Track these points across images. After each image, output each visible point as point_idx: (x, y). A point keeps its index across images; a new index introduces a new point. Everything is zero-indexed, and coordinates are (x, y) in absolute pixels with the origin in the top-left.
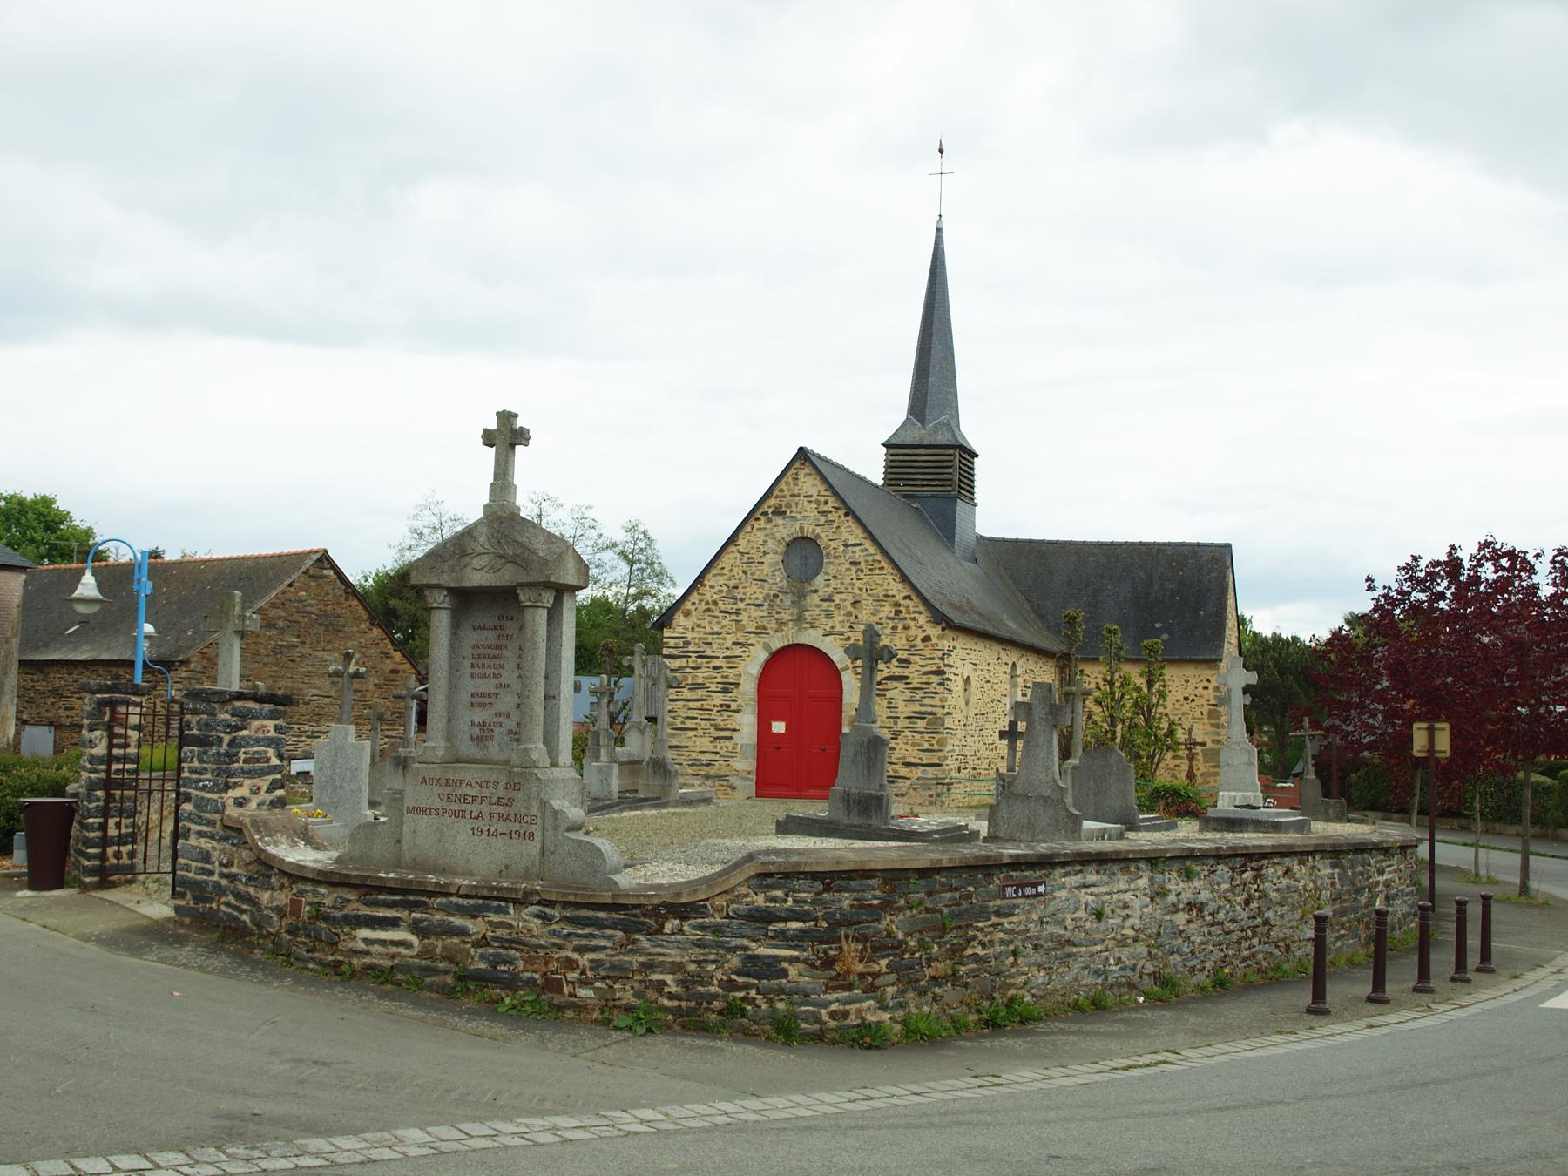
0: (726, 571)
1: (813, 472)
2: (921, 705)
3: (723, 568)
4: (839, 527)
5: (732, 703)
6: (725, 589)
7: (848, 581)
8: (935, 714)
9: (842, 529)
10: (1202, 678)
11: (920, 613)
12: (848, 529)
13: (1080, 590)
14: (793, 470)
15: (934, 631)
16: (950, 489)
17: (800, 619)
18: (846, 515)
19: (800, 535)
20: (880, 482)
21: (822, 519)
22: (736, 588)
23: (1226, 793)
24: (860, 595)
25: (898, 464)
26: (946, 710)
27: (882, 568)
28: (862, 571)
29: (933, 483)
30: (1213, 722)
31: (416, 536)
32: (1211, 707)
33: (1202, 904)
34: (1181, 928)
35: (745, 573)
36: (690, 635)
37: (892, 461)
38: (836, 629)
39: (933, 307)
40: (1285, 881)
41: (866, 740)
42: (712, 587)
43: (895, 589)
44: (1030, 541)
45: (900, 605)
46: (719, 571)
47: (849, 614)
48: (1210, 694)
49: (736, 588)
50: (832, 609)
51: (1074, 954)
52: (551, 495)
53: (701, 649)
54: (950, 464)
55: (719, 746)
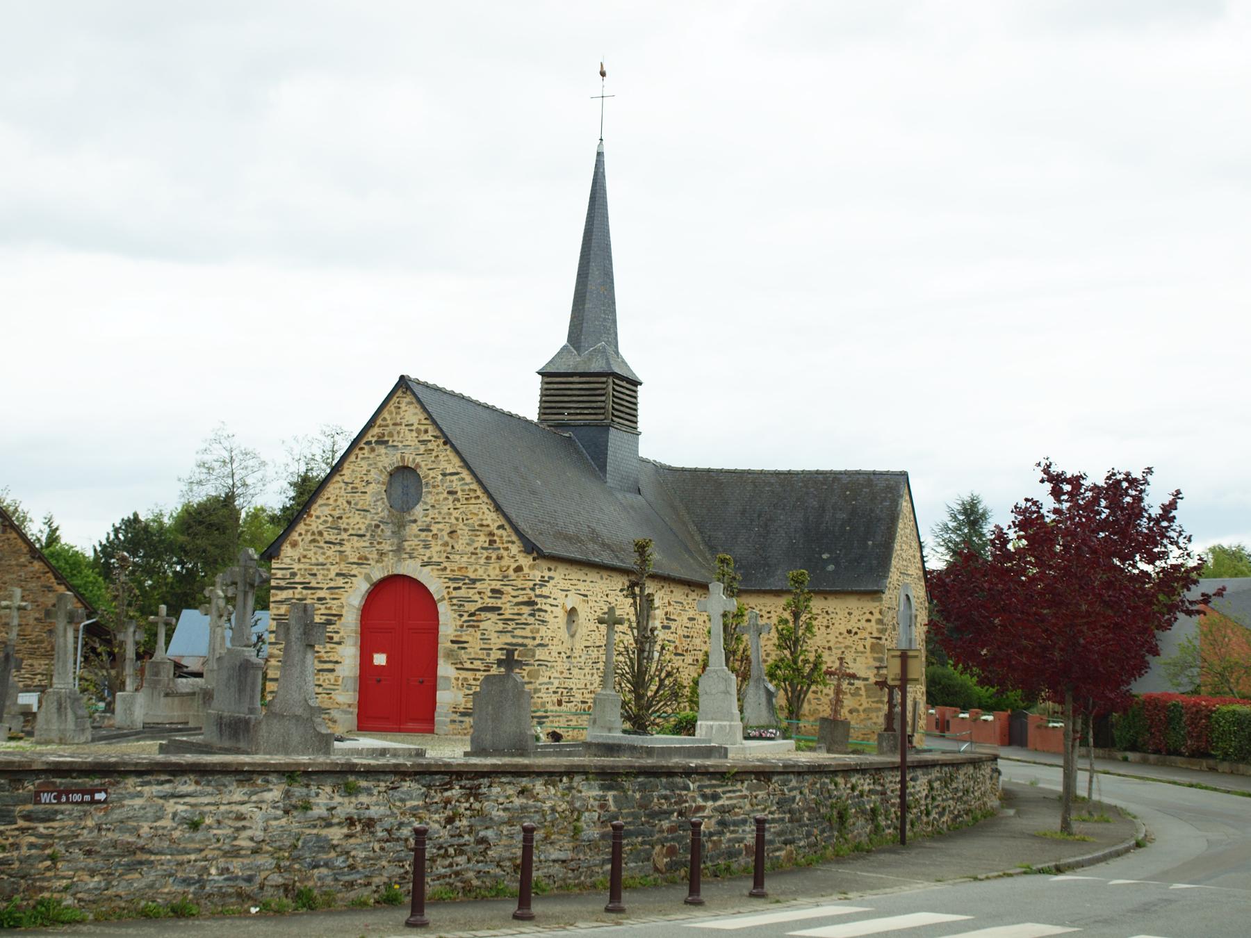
0: (331, 501)
1: (414, 400)
2: (513, 637)
3: (328, 498)
4: (438, 456)
6: (330, 519)
7: (445, 510)
8: (526, 646)
9: (441, 457)
10: (864, 610)
11: (513, 542)
12: (446, 458)
13: (752, 520)
14: (395, 399)
15: (525, 561)
16: (602, 417)
17: (399, 550)
18: (445, 443)
19: (401, 464)
20: (532, 414)
21: (422, 448)
22: (340, 518)
23: (704, 723)
24: (457, 525)
25: (552, 392)
26: (538, 641)
27: (478, 497)
28: (458, 500)
29: (586, 412)
30: (876, 655)
31: (205, 471)
32: (874, 641)
33: (371, 819)
34: (335, 842)
35: (349, 503)
36: (296, 566)
37: (546, 389)
38: (433, 560)
39: (592, 232)
40: (518, 802)
41: (238, 664)
42: (318, 517)
43: (489, 518)
44: (709, 471)
45: (494, 535)
46: (325, 502)
47: (446, 544)
48: (873, 626)
49: (340, 518)
50: (430, 539)
51: (152, 862)
52: (345, 429)
53: (307, 581)
54: (603, 392)
55: (322, 679)
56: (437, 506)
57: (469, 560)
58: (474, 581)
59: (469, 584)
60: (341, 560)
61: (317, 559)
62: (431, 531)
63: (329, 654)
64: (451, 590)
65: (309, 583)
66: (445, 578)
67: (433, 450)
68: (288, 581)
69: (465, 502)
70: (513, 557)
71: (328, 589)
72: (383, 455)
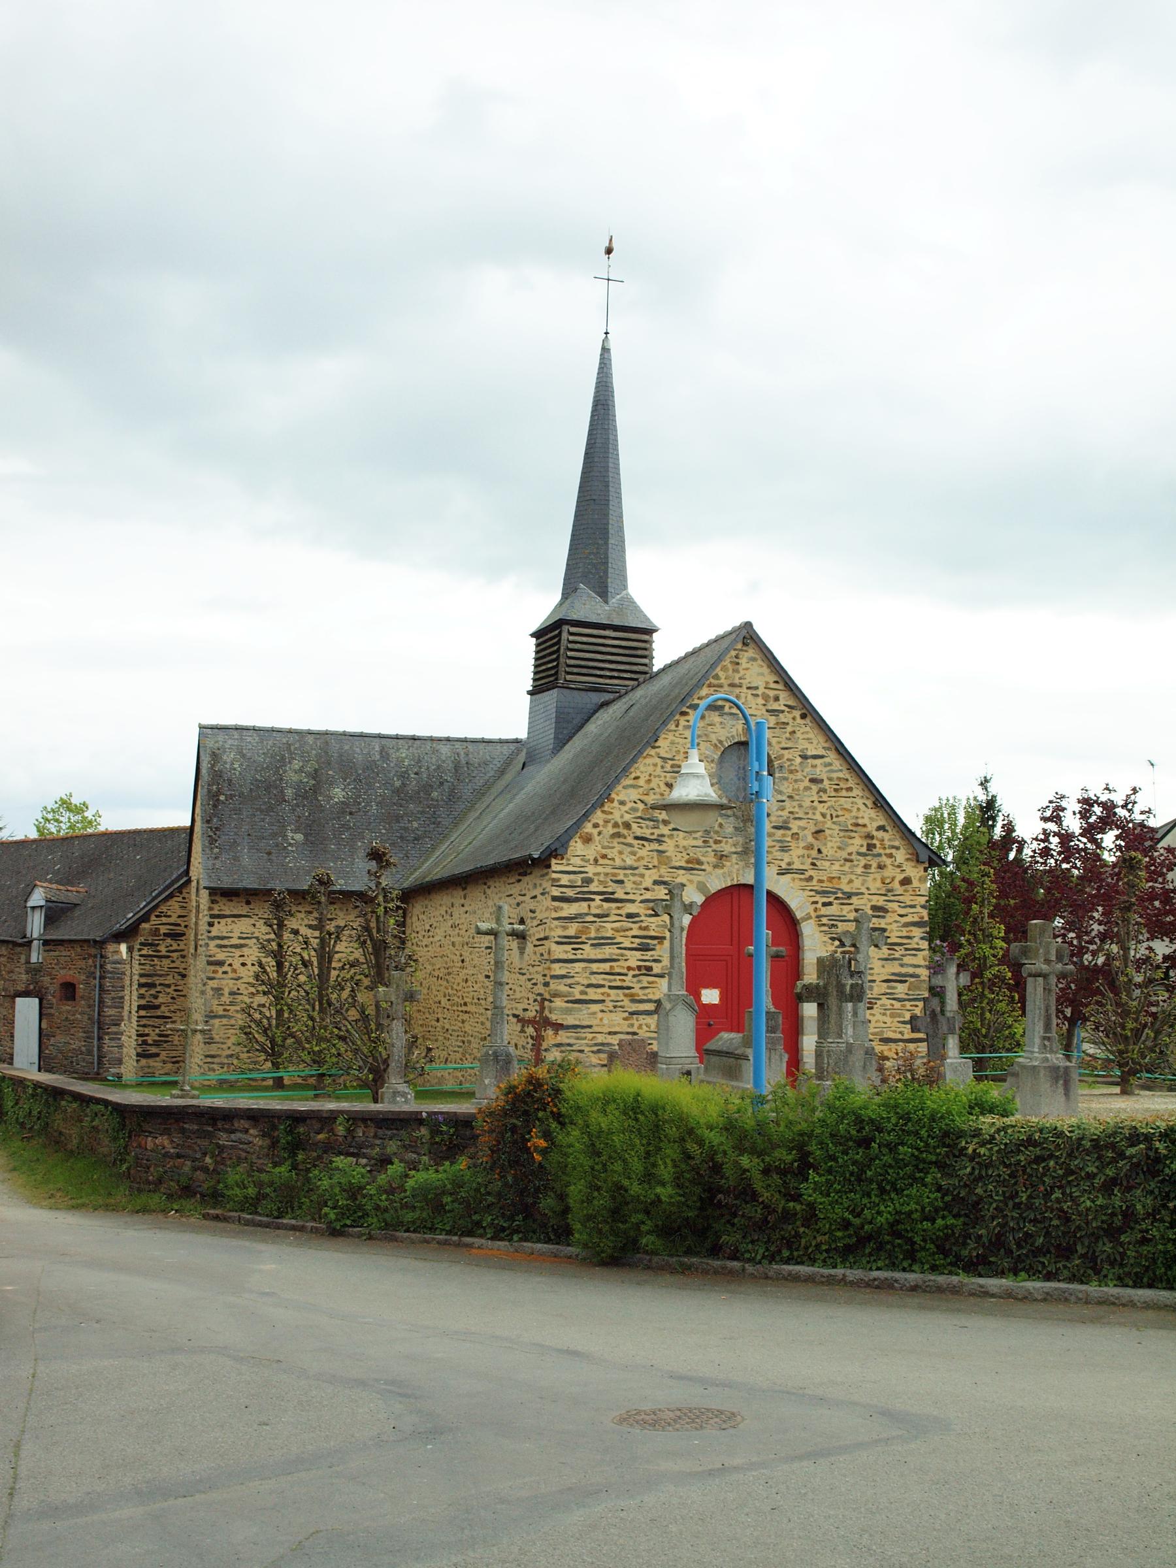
0: (641, 782)
2: (902, 966)
3: (636, 778)
4: (794, 732)
5: (654, 965)
6: (641, 806)
7: (807, 803)
8: (917, 976)
9: (798, 734)
11: (897, 848)
21: (772, 720)
27: (850, 789)
28: (825, 791)
29: (625, 675)
36: (591, 870)
42: (622, 803)
43: (866, 816)
45: (872, 837)
47: (810, 847)
50: (789, 839)
53: (610, 890)
55: (636, 1024)
56: (797, 797)
57: (842, 869)
58: (849, 896)
59: (842, 898)
60: (660, 862)
61: (624, 861)
62: (789, 829)
63: (647, 991)
64: (819, 905)
65: (613, 893)
66: (811, 890)
67: (788, 724)
68: (579, 889)
69: (833, 794)
70: (899, 866)
71: (641, 902)
72: (718, 725)
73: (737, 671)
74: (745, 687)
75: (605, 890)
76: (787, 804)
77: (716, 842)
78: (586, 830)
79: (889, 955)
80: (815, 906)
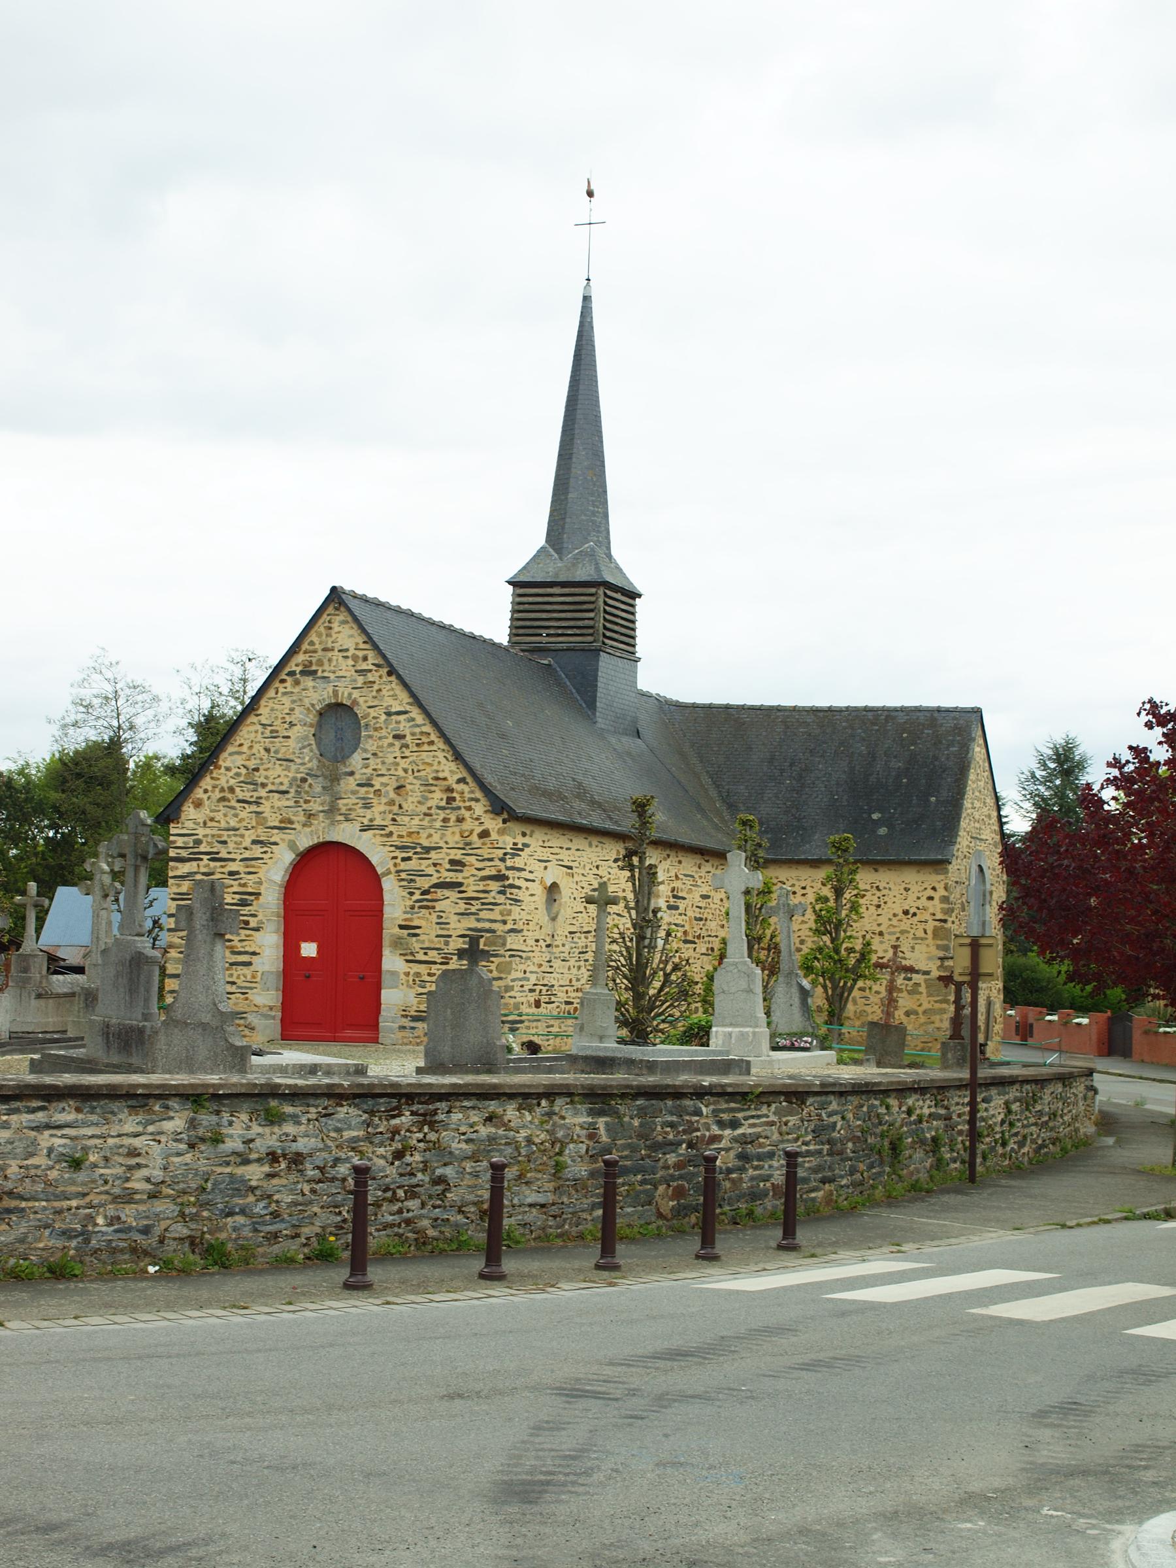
0: (245, 749)
1: (349, 619)
2: (478, 920)
3: (241, 745)
4: (380, 690)
5: (250, 919)
6: (243, 771)
7: (390, 760)
8: (494, 931)
9: (384, 692)
10: (925, 885)
11: (477, 800)
12: (391, 693)
13: (782, 771)
14: (325, 617)
15: (493, 824)
16: (590, 639)
17: (332, 810)
18: (390, 674)
19: (333, 701)
20: (501, 635)
21: (360, 680)
22: (257, 770)
23: (720, 1029)
24: (405, 778)
25: (527, 607)
26: (509, 926)
27: (431, 743)
28: (407, 746)
29: (569, 632)
30: (940, 942)
31: (82, 709)
32: (937, 923)
33: (299, 1154)
34: (253, 1183)
35: (267, 750)
36: (201, 832)
37: (519, 603)
38: (376, 823)
39: (576, 400)
40: (484, 1131)
41: (128, 957)
42: (228, 769)
43: (447, 769)
44: (727, 707)
45: (452, 790)
46: (237, 749)
47: (391, 803)
48: (936, 906)
49: (257, 770)
51: (23, 1210)
52: (258, 653)
53: (215, 850)
54: (591, 606)
55: (235, 974)
56: (380, 754)
57: (421, 823)
58: (428, 850)
59: (421, 853)
60: (257, 823)
61: (228, 823)
62: (372, 786)
63: (244, 943)
64: (398, 861)
65: (218, 853)
66: (391, 846)
67: (374, 682)
68: (191, 850)
69: (415, 749)
70: (477, 819)
71: (241, 860)
72: (311, 690)
73: (328, 635)
74: (336, 650)
75: (211, 850)
76: (371, 761)
77: (306, 802)
78: (198, 796)
79: (466, 909)
80: (395, 861)
